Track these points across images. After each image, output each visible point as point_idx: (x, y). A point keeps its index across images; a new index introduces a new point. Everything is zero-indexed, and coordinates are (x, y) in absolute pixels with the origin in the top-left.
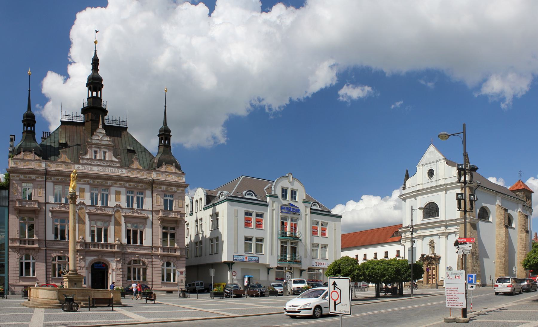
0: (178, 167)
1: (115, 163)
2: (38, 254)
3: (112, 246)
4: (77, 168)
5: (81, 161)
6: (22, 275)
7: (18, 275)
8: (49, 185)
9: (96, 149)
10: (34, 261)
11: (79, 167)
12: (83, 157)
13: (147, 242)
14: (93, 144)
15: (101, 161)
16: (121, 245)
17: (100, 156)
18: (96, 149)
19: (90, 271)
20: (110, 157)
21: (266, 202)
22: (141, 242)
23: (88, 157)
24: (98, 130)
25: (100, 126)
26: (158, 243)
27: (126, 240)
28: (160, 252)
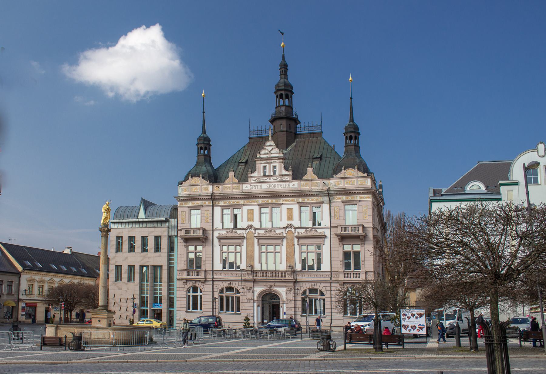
1: (286, 177)
2: (204, 286)
4: (246, 188)
6: (189, 309)
7: (185, 309)
8: (217, 210)
9: (265, 165)
10: (201, 294)
11: (247, 187)
12: (252, 175)
13: (325, 266)
14: (262, 159)
16: (294, 272)
17: (270, 171)
18: (265, 165)
20: (280, 170)
21: (500, 194)
22: (319, 267)
23: (256, 174)
24: (268, 143)
25: (270, 138)
26: (339, 265)
28: (341, 277)
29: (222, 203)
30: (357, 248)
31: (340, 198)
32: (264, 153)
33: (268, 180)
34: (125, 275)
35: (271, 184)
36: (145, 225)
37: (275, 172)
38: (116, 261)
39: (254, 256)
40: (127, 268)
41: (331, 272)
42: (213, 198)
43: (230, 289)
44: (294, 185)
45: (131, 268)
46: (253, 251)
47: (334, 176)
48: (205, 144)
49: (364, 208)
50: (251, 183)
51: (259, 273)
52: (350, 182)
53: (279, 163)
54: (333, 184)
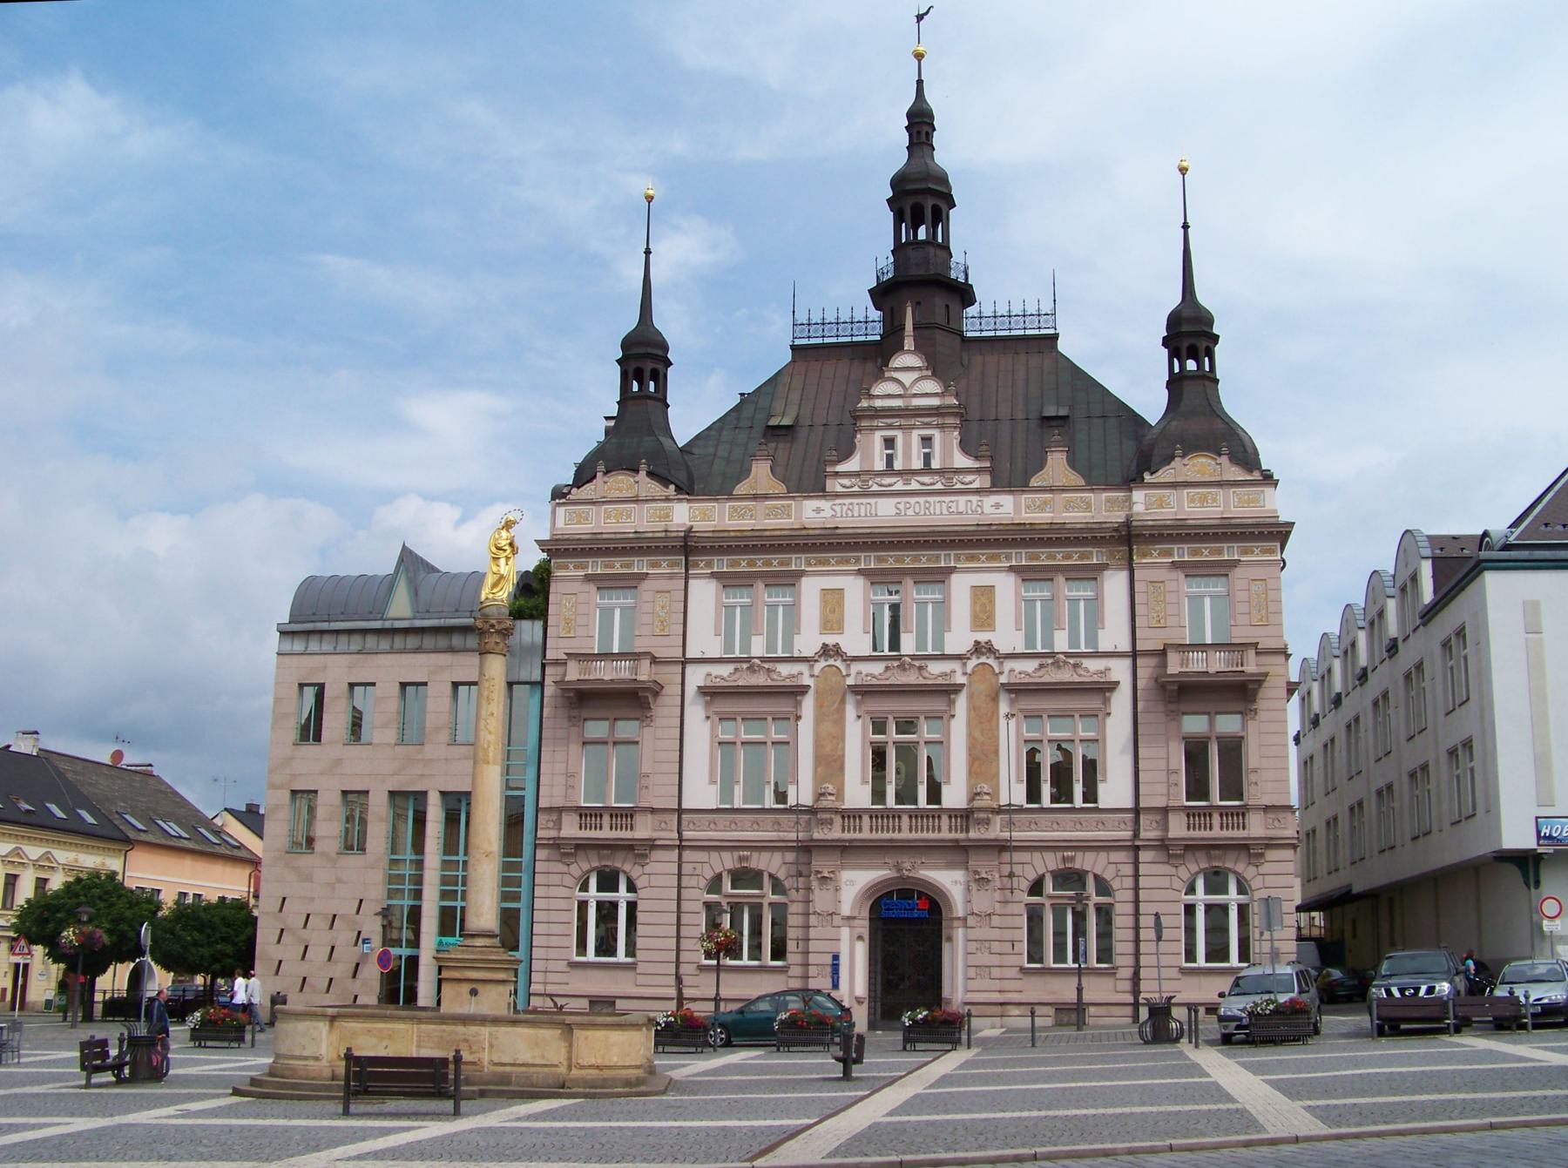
0: (1245, 456)
1: (969, 478)
2: (647, 869)
3: (965, 816)
4: (813, 513)
5: (834, 485)
11: (818, 510)
12: (840, 468)
13: (1115, 791)
14: (877, 413)
15: (910, 469)
19: (866, 933)
20: (946, 454)
22: (1090, 795)
24: (899, 361)
25: (909, 343)
27: (1023, 788)
28: (1178, 828)
29: (722, 564)
30: (1228, 724)
31: (1169, 553)
32: (885, 393)
33: (899, 486)
34: (329, 829)
35: (913, 500)
36: (413, 641)
37: (927, 458)
38: (294, 776)
39: (842, 758)
40: (337, 799)
41: (1137, 811)
42: (688, 547)
43: (746, 877)
44: (997, 506)
45: (354, 799)
46: (840, 738)
47: (1147, 477)
48: (644, 359)
49: (1255, 587)
50: (837, 495)
51: (866, 819)
52: (1203, 500)
53: (941, 427)
54: (1143, 504)
